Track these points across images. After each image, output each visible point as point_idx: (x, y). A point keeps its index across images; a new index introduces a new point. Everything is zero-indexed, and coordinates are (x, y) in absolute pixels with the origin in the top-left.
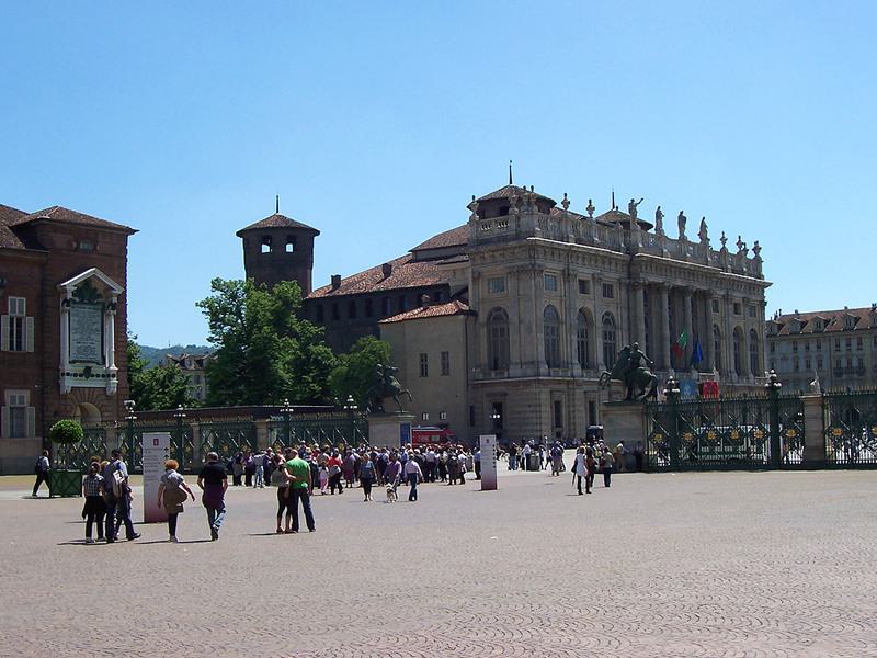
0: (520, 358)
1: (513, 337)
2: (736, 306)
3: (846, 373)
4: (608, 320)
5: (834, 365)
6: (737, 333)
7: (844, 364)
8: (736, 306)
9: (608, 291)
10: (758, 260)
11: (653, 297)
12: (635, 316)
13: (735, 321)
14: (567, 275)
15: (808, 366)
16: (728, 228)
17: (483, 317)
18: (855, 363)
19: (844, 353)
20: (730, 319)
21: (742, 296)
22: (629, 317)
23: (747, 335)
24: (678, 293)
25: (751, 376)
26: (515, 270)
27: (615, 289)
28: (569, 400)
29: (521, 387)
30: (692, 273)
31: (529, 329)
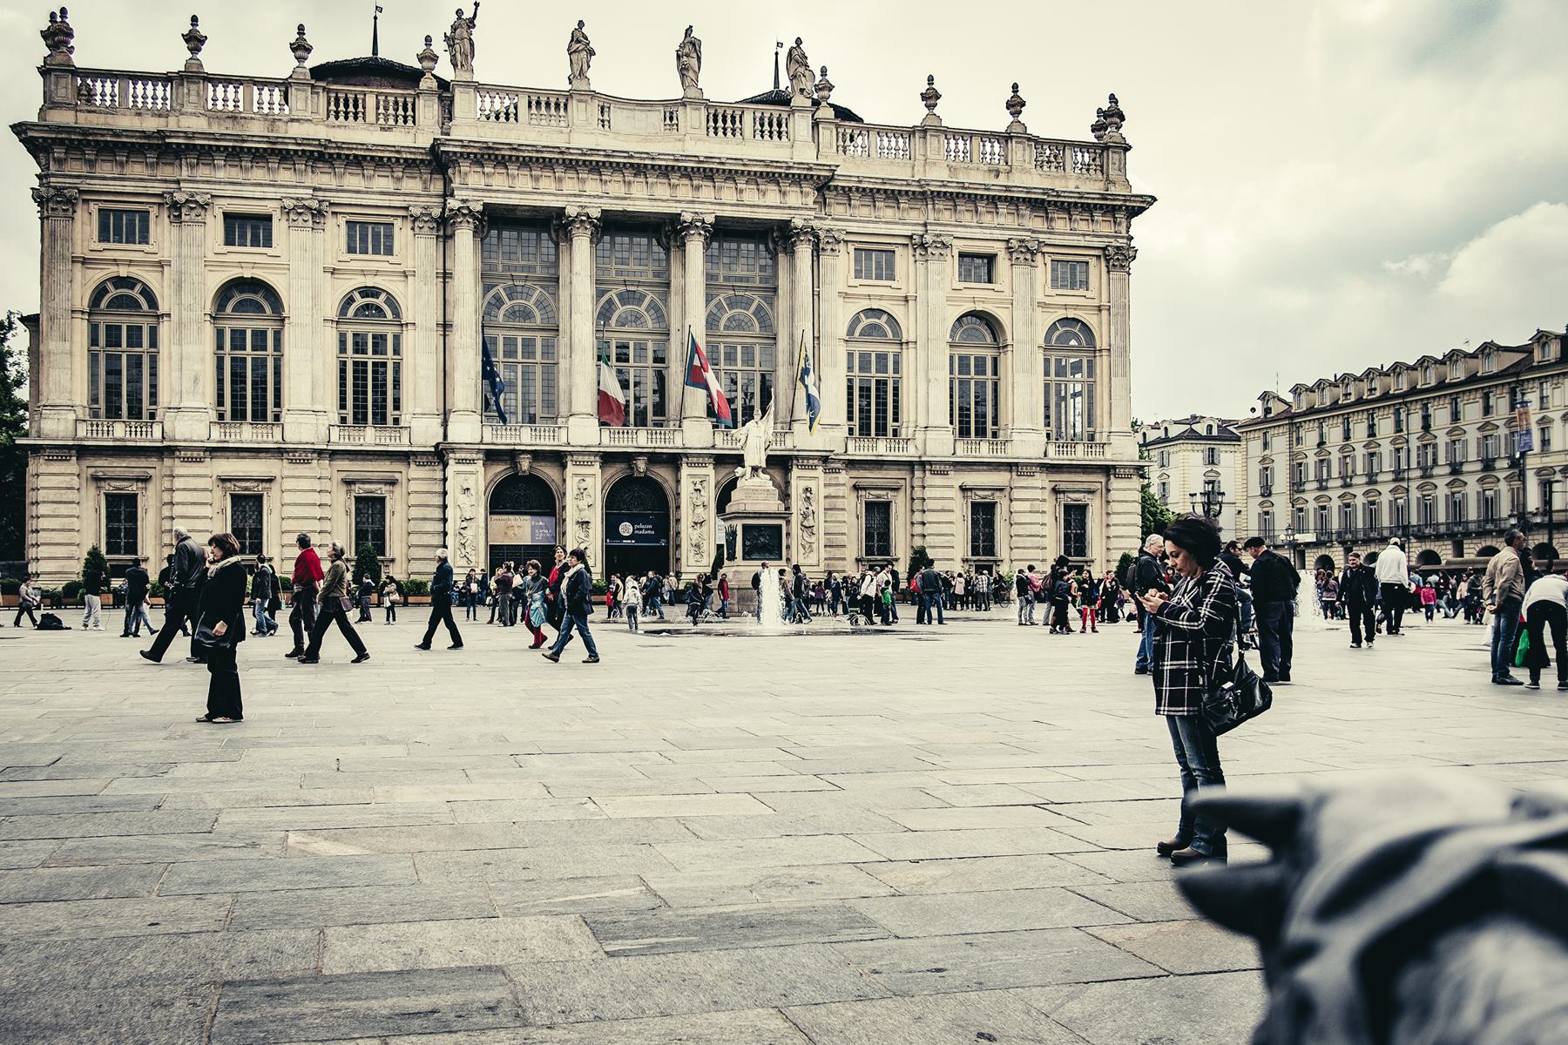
9: (369, 236)
20: (937, 296)
21: (997, 234)
27: (402, 234)
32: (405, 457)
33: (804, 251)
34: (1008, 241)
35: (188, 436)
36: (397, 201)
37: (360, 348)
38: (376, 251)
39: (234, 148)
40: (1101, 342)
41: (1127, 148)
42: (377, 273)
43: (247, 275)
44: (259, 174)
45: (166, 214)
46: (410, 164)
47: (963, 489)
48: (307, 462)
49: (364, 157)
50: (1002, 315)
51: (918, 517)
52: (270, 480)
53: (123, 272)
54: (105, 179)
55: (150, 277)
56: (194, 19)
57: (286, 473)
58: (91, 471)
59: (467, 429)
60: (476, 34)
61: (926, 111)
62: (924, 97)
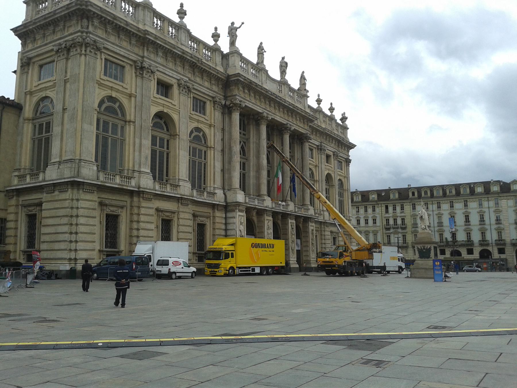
3: (394, 228)
4: (198, 137)
6: (329, 178)
7: (391, 222)
8: (328, 157)
9: (199, 106)
10: (345, 128)
11: (251, 127)
12: (230, 139)
15: (367, 222)
16: (327, 92)
18: (399, 222)
19: (391, 215)
20: (323, 166)
22: (223, 140)
23: (336, 183)
24: (275, 129)
26: (63, 46)
28: (132, 214)
29: (56, 193)
30: (291, 111)
31: (73, 118)
32: (213, 206)
33: (307, 145)
35: (145, 187)
36: (211, 94)
37: (194, 155)
38: (200, 113)
39: (169, 49)
40: (345, 187)
41: (348, 129)
42: (202, 122)
43: (165, 111)
44: (171, 65)
45: (134, 70)
46: (218, 79)
47: (332, 232)
48: (187, 205)
49: (207, 71)
50: (333, 175)
51: (323, 241)
52: (174, 213)
53: (114, 95)
54: (113, 44)
55: (125, 101)
57: (181, 210)
58: (100, 200)
59: (240, 197)
60: (237, 33)
61: (317, 106)
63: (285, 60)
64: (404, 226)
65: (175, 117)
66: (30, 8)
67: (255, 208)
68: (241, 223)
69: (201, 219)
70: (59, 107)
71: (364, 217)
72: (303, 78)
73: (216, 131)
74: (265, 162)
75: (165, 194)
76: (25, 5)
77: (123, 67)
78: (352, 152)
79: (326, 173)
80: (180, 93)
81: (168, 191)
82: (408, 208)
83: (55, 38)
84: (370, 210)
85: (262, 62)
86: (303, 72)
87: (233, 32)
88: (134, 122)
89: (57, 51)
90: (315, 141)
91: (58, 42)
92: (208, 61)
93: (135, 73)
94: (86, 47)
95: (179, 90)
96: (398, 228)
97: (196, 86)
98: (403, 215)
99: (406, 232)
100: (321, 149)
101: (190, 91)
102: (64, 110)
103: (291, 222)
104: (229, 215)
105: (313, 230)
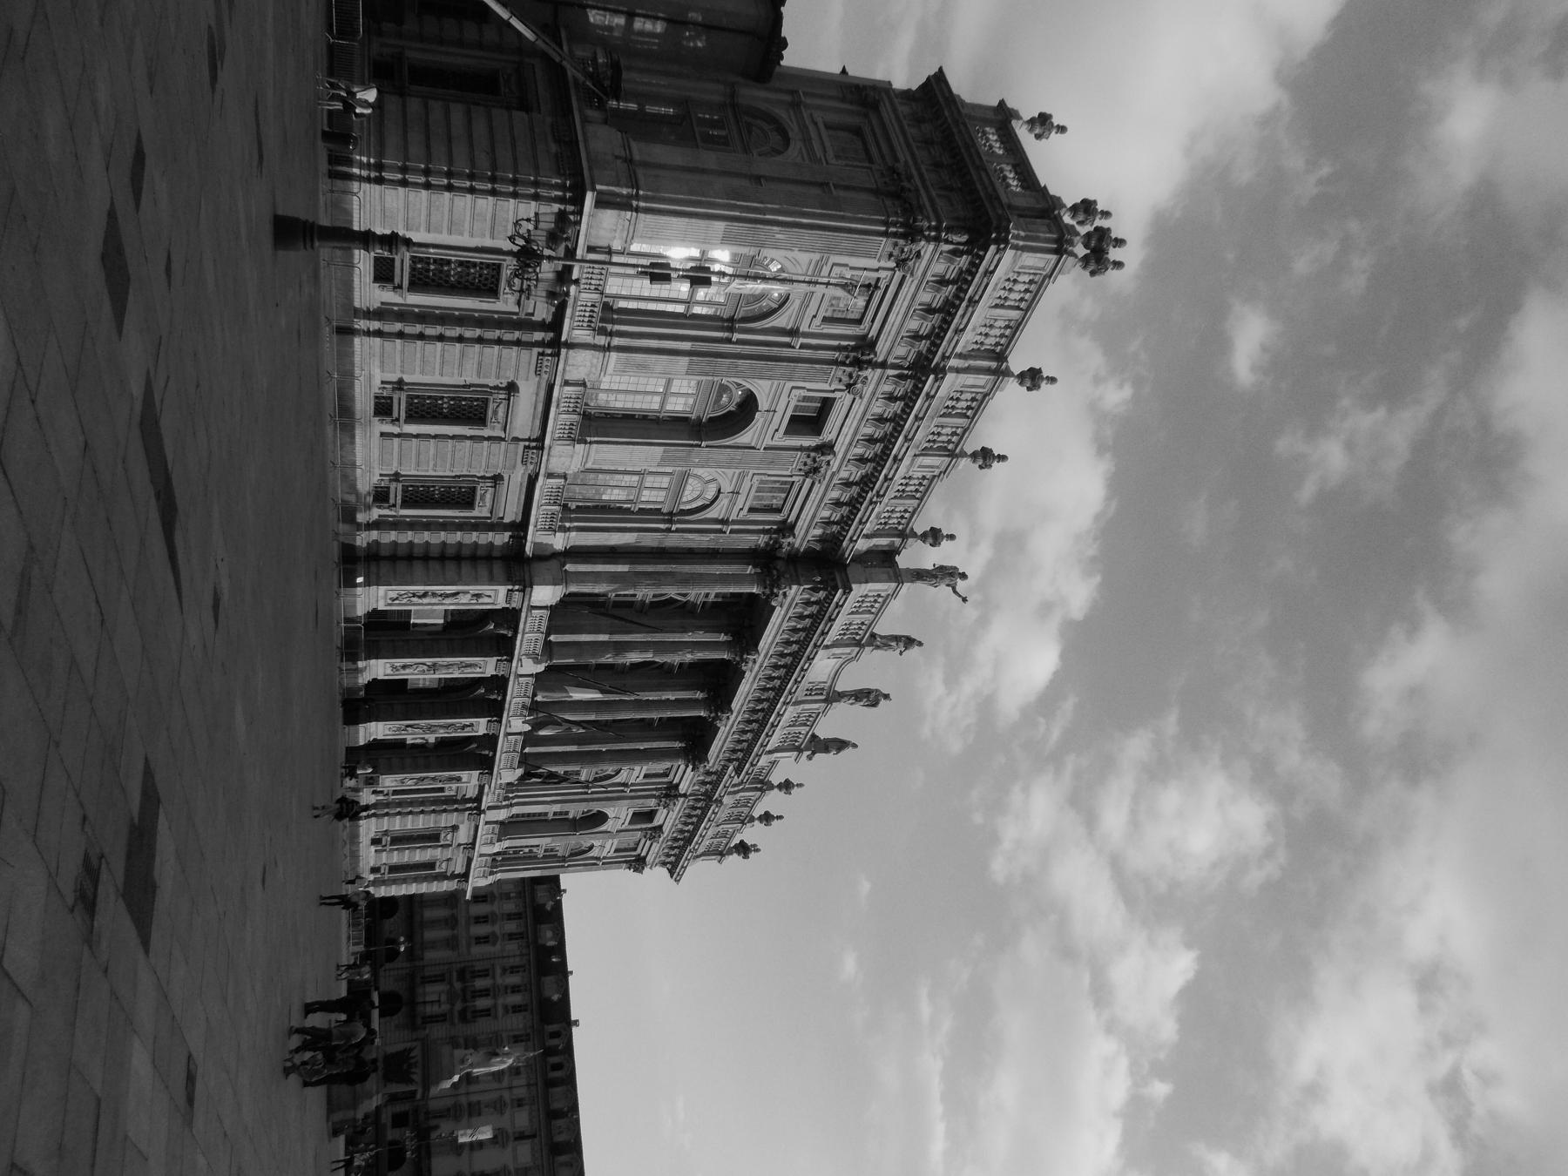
0: (645, 165)
1: (710, 159)
2: (649, 815)
3: (464, 990)
5: (479, 966)
7: (480, 983)
10: (720, 853)
13: (619, 814)
14: (860, 354)
17: (753, 95)
18: (482, 1003)
24: (718, 682)
25: (497, 848)
26: (906, 184)
29: (554, 148)
30: (760, 718)
33: (681, 763)
34: (660, 827)
42: (732, 503)
47: (455, 828)
50: (603, 828)
56: (1052, 380)
62: (787, 781)
63: (883, 702)
64: (469, 1015)
65: (745, 437)
66: (990, 115)
67: (516, 632)
68: (478, 596)
69: (488, 496)
70: (764, 167)
71: (493, 913)
72: (840, 745)
73: (712, 536)
74: (634, 657)
75: (553, 409)
76: (995, 103)
77: (859, 322)
78: (664, 871)
79: (610, 812)
80: (801, 449)
81: (560, 419)
82: (517, 1022)
83: (923, 168)
84: (511, 927)
85: (878, 647)
86: (855, 746)
87: (947, 574)
88: (729, 341)
89: (893, 170)
90: (688, 779)
91: (914, 172)
92: (878, 517)
93: (845, 348)
94: (903, 236)
95: (809, 449)
96: (465, 1000)
97: (818, 490)
98: (500, 1011)
99: (453, 1024)
100: (666, 796)
101: (806, 475)
102: (758, 179)
103: (481, 726)
104: (498, 568)
105: (459, 779)
